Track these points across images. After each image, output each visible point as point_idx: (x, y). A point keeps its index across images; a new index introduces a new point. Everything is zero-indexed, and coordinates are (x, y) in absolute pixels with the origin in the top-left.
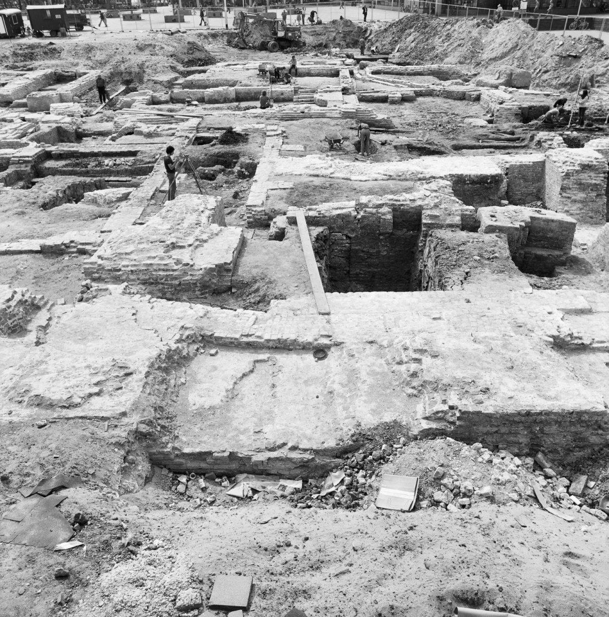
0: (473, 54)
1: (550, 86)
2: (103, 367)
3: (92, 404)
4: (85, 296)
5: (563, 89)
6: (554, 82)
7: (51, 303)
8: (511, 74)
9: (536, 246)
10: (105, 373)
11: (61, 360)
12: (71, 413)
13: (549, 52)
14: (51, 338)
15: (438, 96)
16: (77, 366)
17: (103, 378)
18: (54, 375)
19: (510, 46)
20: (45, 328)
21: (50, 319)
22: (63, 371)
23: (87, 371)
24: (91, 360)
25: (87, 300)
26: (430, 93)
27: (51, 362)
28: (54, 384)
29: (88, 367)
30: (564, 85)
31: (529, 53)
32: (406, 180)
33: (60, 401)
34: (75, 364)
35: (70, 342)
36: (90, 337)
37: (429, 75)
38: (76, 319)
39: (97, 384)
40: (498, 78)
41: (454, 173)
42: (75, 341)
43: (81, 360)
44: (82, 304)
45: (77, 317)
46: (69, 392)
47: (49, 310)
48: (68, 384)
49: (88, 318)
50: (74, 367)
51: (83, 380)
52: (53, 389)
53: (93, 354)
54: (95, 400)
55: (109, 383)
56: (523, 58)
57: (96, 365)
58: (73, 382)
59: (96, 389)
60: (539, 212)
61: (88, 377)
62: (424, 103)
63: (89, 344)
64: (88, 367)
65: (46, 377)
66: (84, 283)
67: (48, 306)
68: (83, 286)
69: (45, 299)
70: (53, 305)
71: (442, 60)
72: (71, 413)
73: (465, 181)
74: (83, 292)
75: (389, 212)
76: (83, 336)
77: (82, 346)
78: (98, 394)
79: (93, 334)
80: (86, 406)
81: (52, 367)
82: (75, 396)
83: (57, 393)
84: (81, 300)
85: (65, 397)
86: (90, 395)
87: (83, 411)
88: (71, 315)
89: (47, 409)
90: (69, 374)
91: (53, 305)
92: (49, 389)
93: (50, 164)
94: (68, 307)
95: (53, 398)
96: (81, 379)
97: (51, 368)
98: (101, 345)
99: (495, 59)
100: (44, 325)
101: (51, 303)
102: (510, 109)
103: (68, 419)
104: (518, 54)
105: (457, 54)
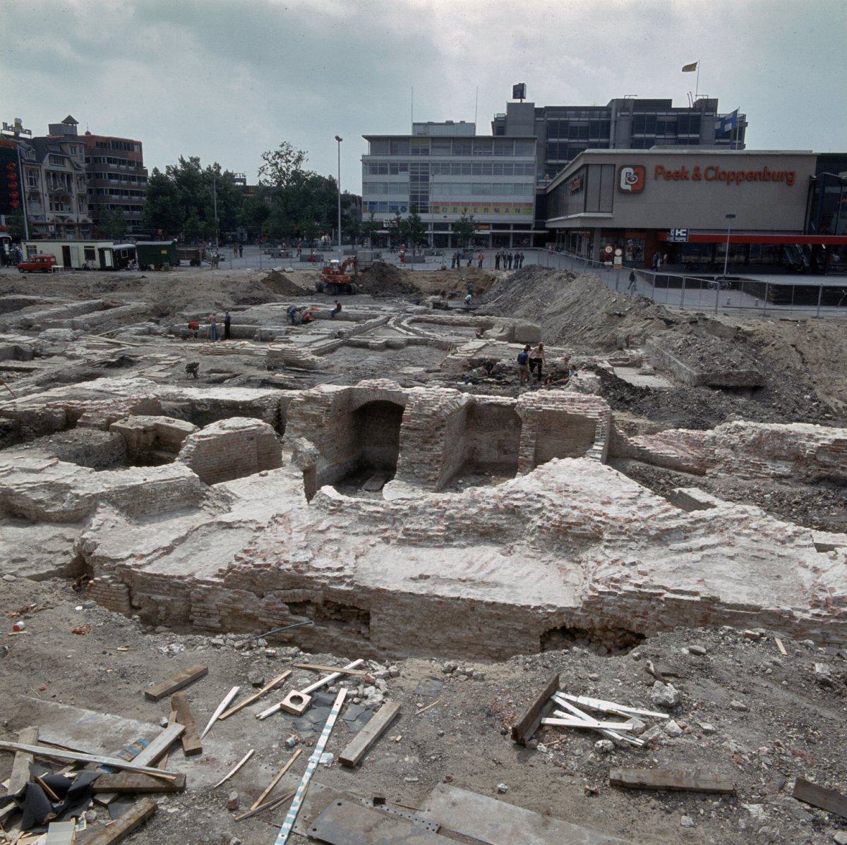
0: (540, 306)
1: (587, 345)
5: (599, 349)
6: (592, 341)
8: (514, 328)
9: (165, 450)
13: (603, 309)
15: (431, 345)
19: (571, 300)
26: (425, 343)
30: (601, 344)
31: (586, 309)
32: (169, 400)
37: (476, 326)
40: (502, 331)
41: (211, 397)
56: (578, 314)
60: (168, 421)
62: (412, 350)
71: (512, 312)
73: (220, 406)
75: (60, 412)
99: (553, 314)
102: (458, 360)
104: (577, 308)
105: (526, 307)
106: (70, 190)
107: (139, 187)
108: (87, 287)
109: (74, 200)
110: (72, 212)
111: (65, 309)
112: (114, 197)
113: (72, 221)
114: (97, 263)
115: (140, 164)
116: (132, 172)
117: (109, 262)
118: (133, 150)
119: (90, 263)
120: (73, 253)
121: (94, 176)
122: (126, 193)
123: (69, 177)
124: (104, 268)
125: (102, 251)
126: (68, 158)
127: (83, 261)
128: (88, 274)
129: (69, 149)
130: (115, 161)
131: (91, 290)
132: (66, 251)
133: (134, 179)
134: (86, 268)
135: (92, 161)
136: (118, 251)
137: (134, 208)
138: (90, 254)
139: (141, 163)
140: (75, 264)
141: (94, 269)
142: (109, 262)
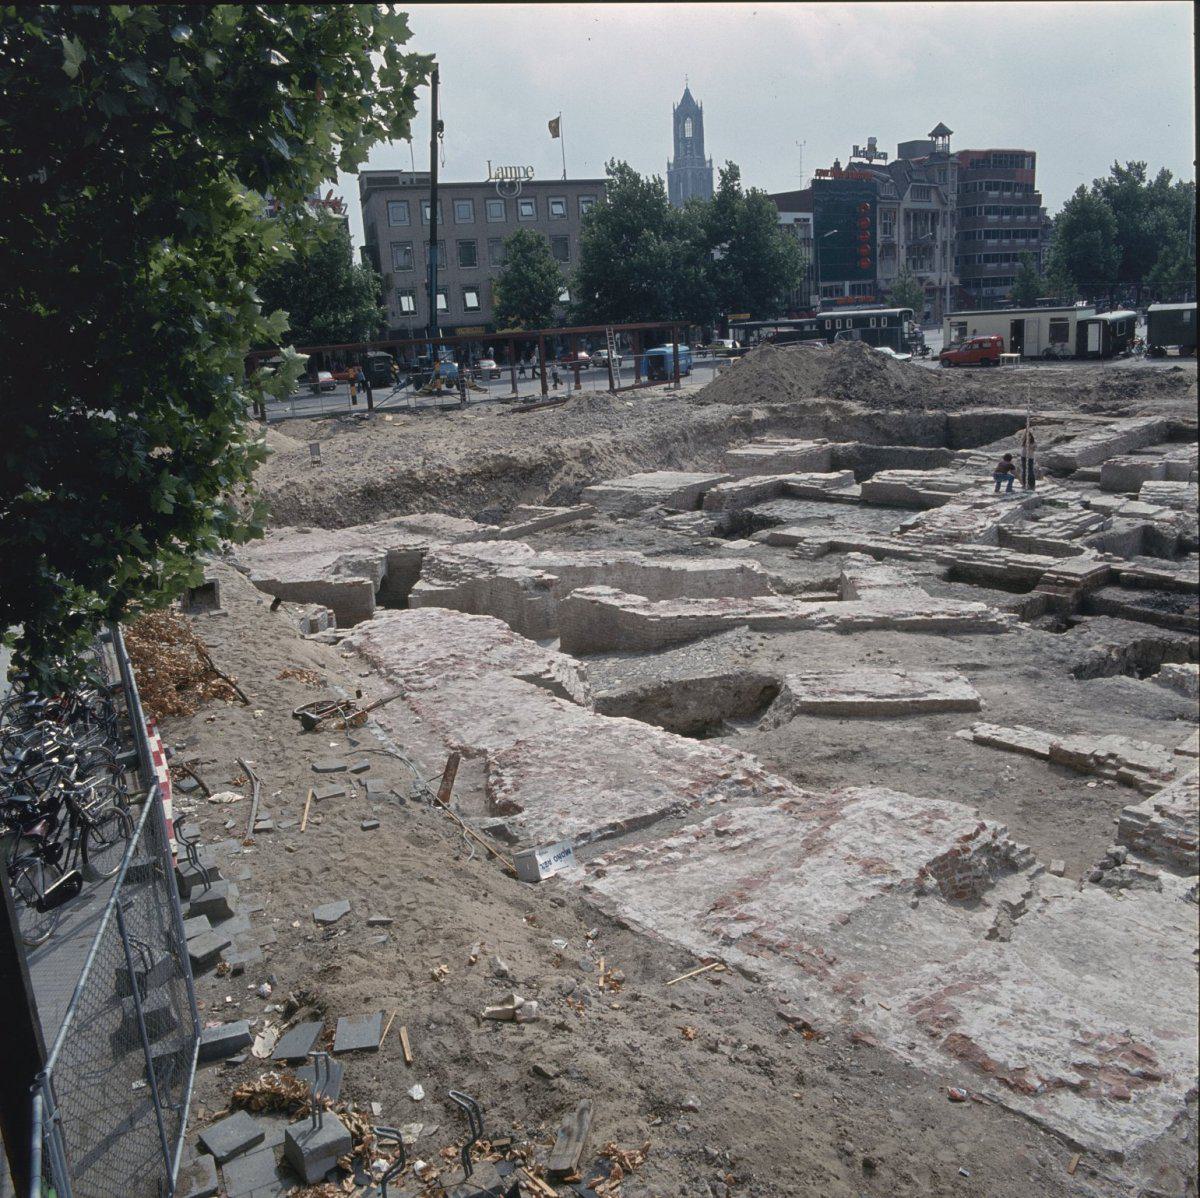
2: (1101, 1037)
3: (1056, 1102)
4: (1107, 875)
7: (1039, 865)
10: (1102, 1052)
11: (1026, 988)
12: (1016, 1102)
14: (1020, 938)
16: (1053, 1013)
17: (1096, 1061)
18: (1005, 1012)
20: (1015, 911)
21: (1028, 895)
22: (1023, 1012)
23: (1068, 1033)
24: (1082, 1013)
25: (1108, 885)
27: (1008, 985)
28: (1002, 1029)
29: (1073, 1025)
33: (1003, 1066)
34: (1051, 1008)
35: (1053, 959)
36: (1093, 965)
38: (1075, 918)
39: (1080, 1067)
42: (1061, 960)
43: (1063, 1003)
44: (1099, 891)
45: (1079, 913)
46: (1023, 1058)
47: (1031, 877)
48: (1026, 1044)
49: (1099, 924)
50: (1046, 1012)
51: (1055, 1047)
52: (996, 1039)
53: (1090, 1002)
54: (1067, 1097)
55: (1104, 1078)
57: (1089, 1029)
58: (1036, 1041)
59: (1076, 1078)
61: (1067, 1045)
63: (1088, 977)
64: (1073, 1025)
65: (990, 1009)
66: (1114, 849)
67: (1033, 869)
68: (1109, 856)
69: (1031, 856)
70: (1041, 871)
72: (1016, 1102)
74: (1104, 867)
76: (1082, 955)
77: (1073, 977)
78: (1077, 1089)
79: (1100, 961)
80: (1047, 1102)
81: (1006, 991)
82: (1031, 1071)
83: (1001, 1050)
84: (1096, 880)
85: (1012, 1064)
86: (1061, 1084)
87: (1038, 1108)
88: (1069, 906)
89: (975, 1071)
90: (1032, 1023)
91: (1041, 871)
92: (988, 1034)
93: (1110, 594)
94: (1067, 885)
95: (991, 1056)
96: (1053, 1042)
97: (1004, 996)
98: (1111, 989)
100: (1015, 902)
101: (1039, 865)
103: (1007, 1110)
106: (934, 237)
107: (1028, 222)
108: (1088, 391)
109: (937, 252)
110: (932, 270)
111: (1113, 437)
112: (992, 242)
113: (930, 283)
114: (1071, 346)
115: (1029, 187)
116: (1019, 201)
117: (1094, 343)
118: (1023, 167)
119: (1057, 349)
120: (1029, 333)
121: (967, 214)
122: (1007, 234)
123: (935, 216)
124: (1082, 355)
125: (1083, 325)
126: (936, 188)
127: (1046, 344)
128: (1064, 368)
129: (937, 174)
130: (996, 186)
131: (1094, 396)
132: (1018, 328)
133: (1019, 212)
134: (1049, 357)
135: (965, 191)
136: (1114, 322)
137: (1007, 258)
138: (1058, 331)
139: (1033, 186)
140: (1030, 349)
141: (1065, 358)
142: (1094, 343)
